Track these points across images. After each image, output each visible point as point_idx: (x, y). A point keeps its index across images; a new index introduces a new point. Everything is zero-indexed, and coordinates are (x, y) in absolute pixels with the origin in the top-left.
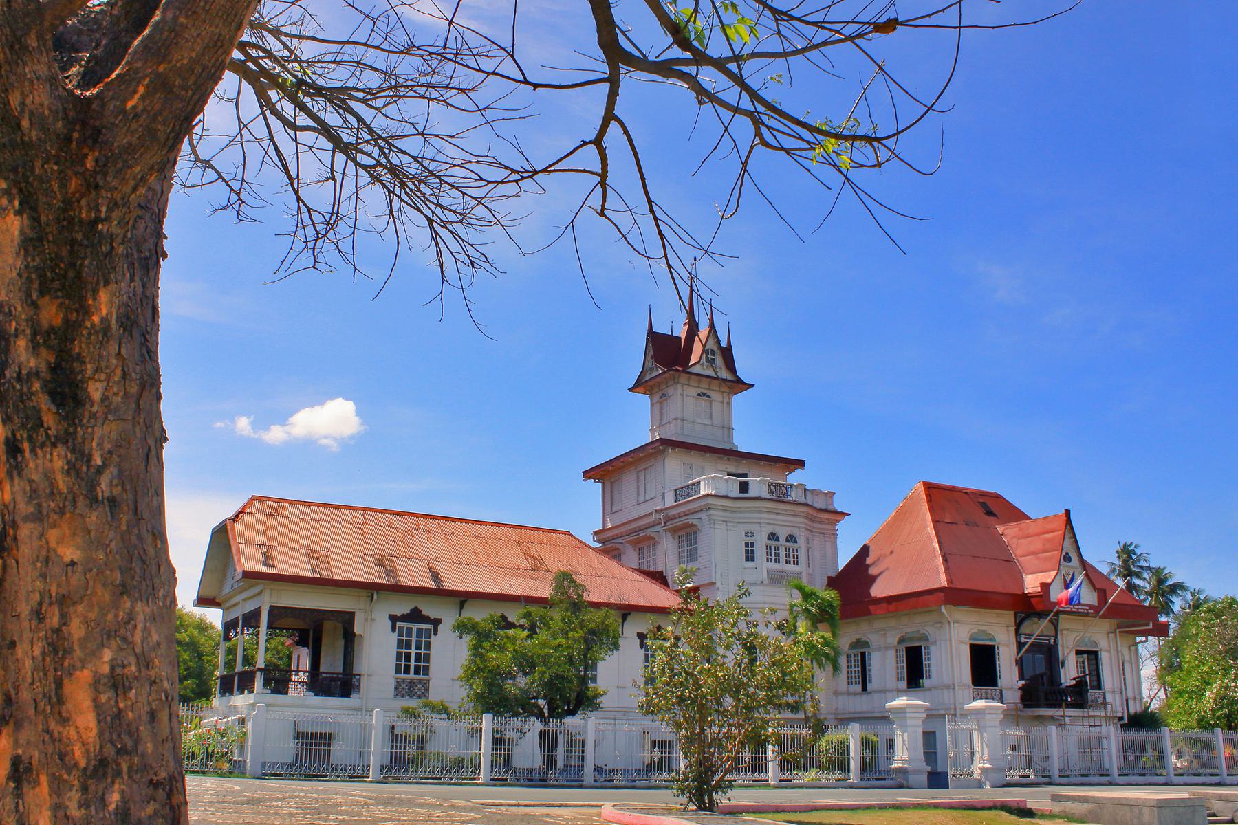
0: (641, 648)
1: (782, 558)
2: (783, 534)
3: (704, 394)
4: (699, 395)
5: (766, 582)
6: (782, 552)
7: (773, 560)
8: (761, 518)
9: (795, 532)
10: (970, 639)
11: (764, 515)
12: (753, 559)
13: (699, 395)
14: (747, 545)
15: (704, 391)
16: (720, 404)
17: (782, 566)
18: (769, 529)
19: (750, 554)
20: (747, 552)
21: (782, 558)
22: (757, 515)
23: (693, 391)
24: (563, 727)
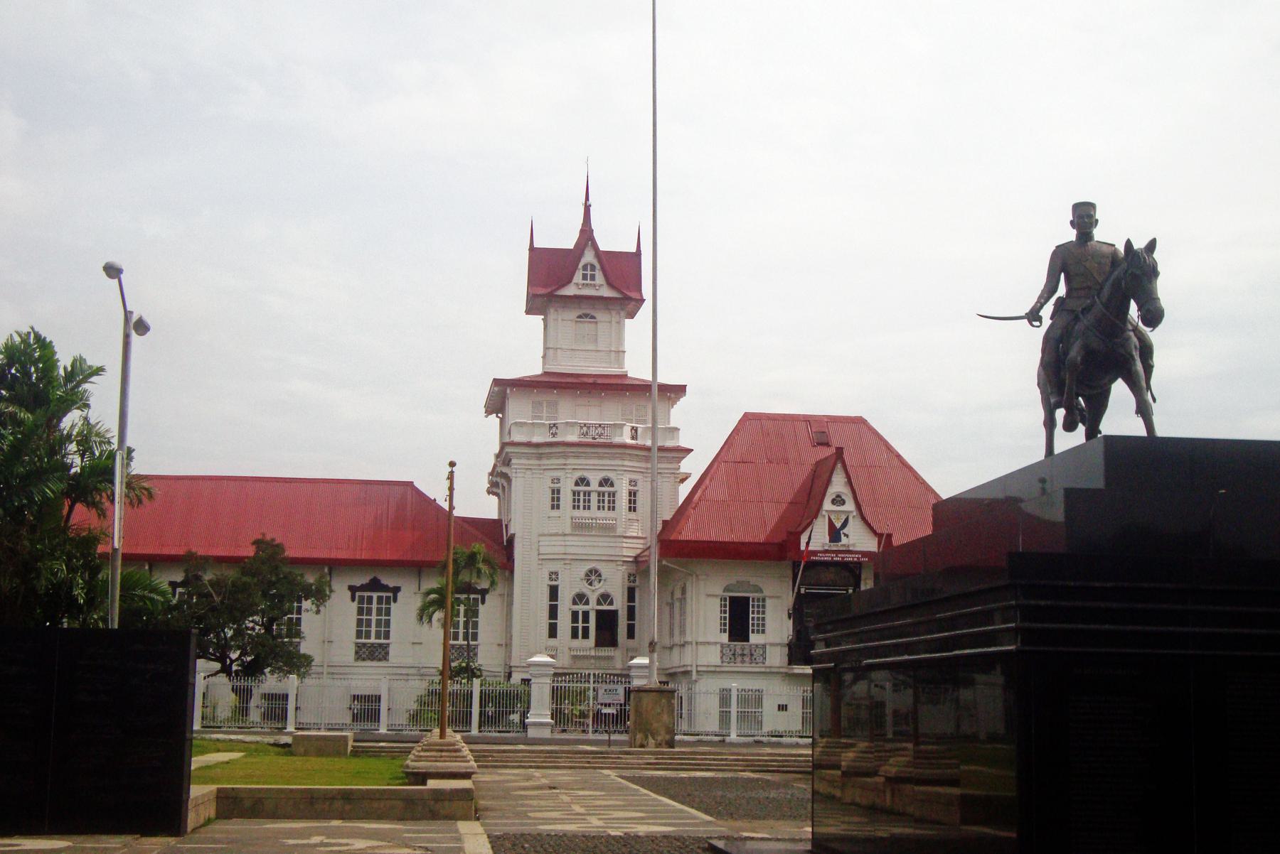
1: (594, 503)
2: (594, 479)
3: (586, 316)
4: (580, 317)
5: (568, 531)
6: (594, 497)
7: (581, 507)
8: (565, 464)
9: (611, 475)
10: (724, 591)
11: (570, 461)
12: (558, 507)
13: (580, 317)
14: (553, 492)
15: (585, 311)
16: (608, 324)
17: (594, 512)
18: (578, 474)
19: (555, 506)
20: (553, 499)
21: (594, 503)
22: (561, 461)
23: (572, 314)
24: (246, 683)
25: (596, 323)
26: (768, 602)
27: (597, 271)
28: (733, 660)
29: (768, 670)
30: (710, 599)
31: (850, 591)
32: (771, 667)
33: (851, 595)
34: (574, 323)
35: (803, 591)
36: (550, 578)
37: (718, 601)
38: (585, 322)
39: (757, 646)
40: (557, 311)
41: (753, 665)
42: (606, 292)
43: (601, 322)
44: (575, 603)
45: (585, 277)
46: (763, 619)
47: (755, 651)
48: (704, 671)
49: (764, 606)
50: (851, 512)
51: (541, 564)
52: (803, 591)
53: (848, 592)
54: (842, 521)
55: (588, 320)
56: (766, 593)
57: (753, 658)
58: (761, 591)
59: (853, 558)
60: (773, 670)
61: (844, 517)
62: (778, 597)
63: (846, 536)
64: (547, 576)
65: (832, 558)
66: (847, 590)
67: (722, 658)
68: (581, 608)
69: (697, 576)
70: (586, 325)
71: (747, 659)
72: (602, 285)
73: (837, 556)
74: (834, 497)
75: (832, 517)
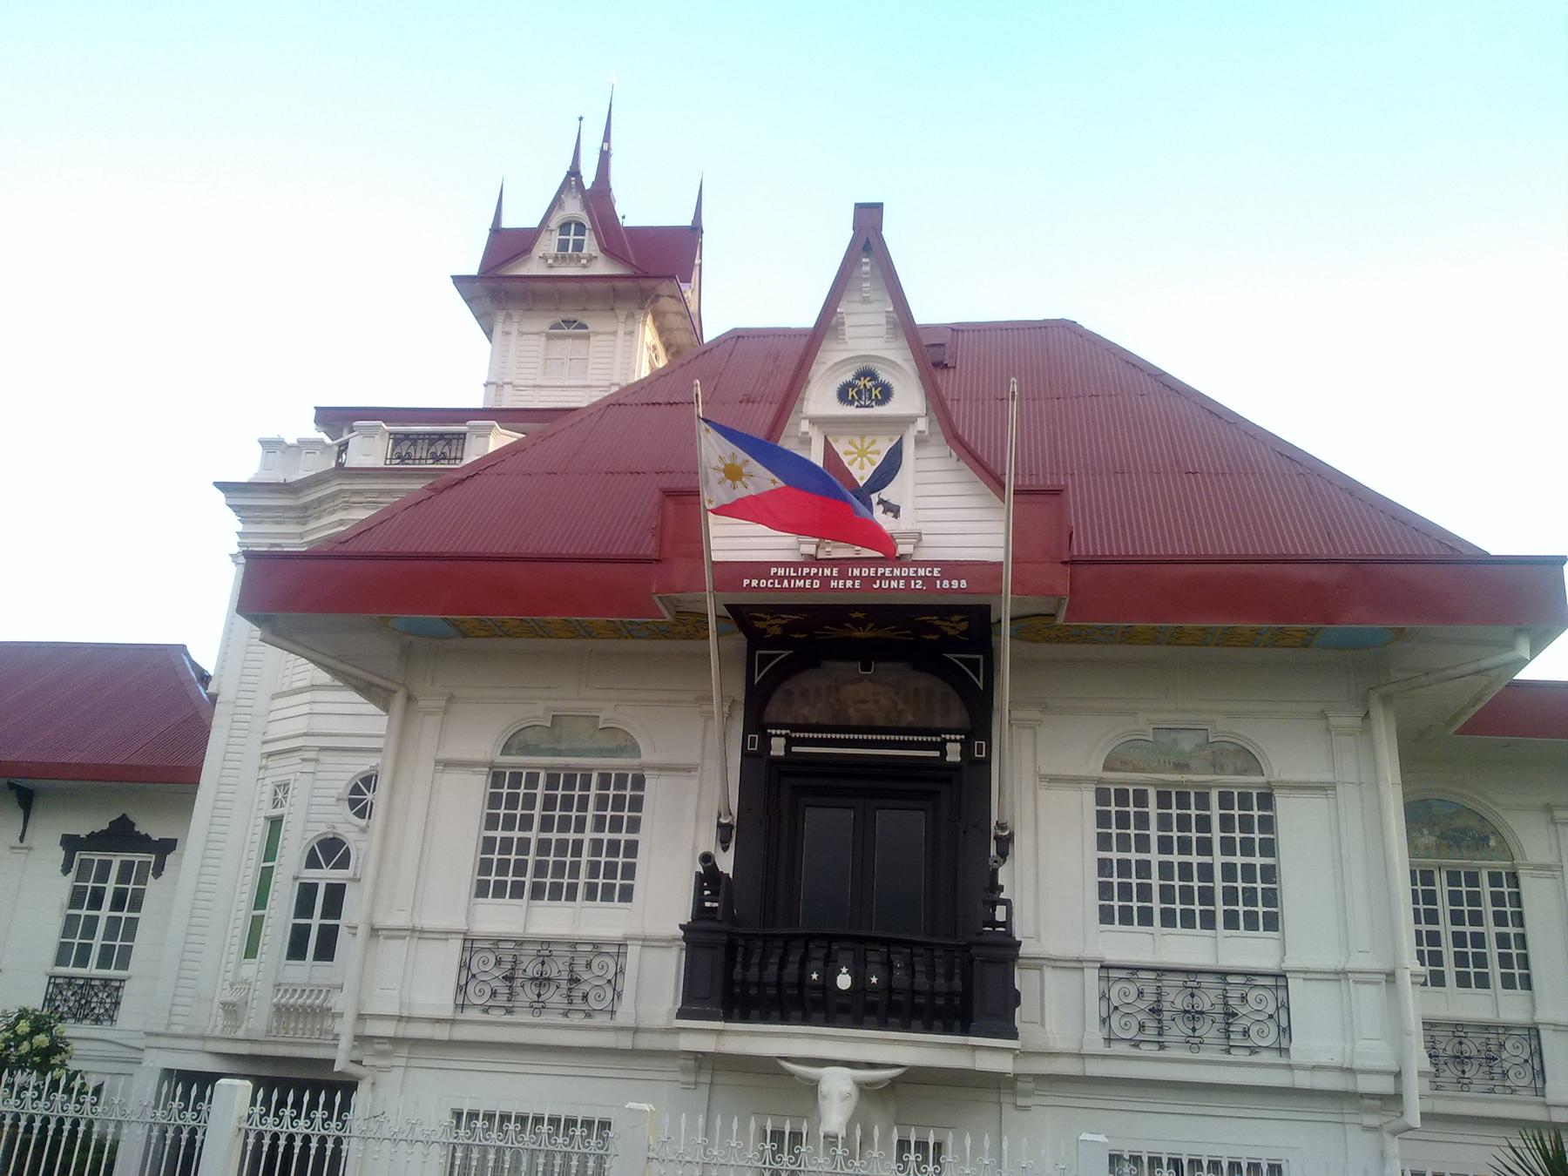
0: (66, 869)
3: (568, 323)
10: (506, 750)
15: (570, 316)
23: (542, 323)
25: (587, 337)
26: (653, 788)
27: (587, 232)
28: (502, 999)
29: (625, 1042)
30: (453, 778)
31: (954, 753)
32: (636, 1030)
33: (954, 766)
34: (543, 339)
35: (778, 747)
36: (274, 800)
37: (476, 787)
38: (569, 336)
39: (596, 945)
40: (508, 316)
41: (577, 1019)
42: (602, 268)
43: (597, 334)
44: (312, 862)
45: (563, 245)
46: (632, 848)
47: (589, 965)
48: (395, 1041)
49: (637, 804)
50: (910, 420)
51: (265, 768)
52: (778, 747)
53: (944, 753)
54: (879, 459)
55: (571, 331)
56: (648, 757)
57: (578, 993)
58: (634, 750)
59: (908, 579)
60: (645, 1042)
61: (884, 446)
62: (687, 769)
63: (893, 510)
64: (268, 797)
65: (825, 581)
66: (941, 747)
67: (461, 989)
68: (325, 876)
69: (410, 699)
70: (570, 341)
71: (555, 997)
72: (596, 257)
73: (843, 576)
74: (849, 377)
75: (840, 447)
